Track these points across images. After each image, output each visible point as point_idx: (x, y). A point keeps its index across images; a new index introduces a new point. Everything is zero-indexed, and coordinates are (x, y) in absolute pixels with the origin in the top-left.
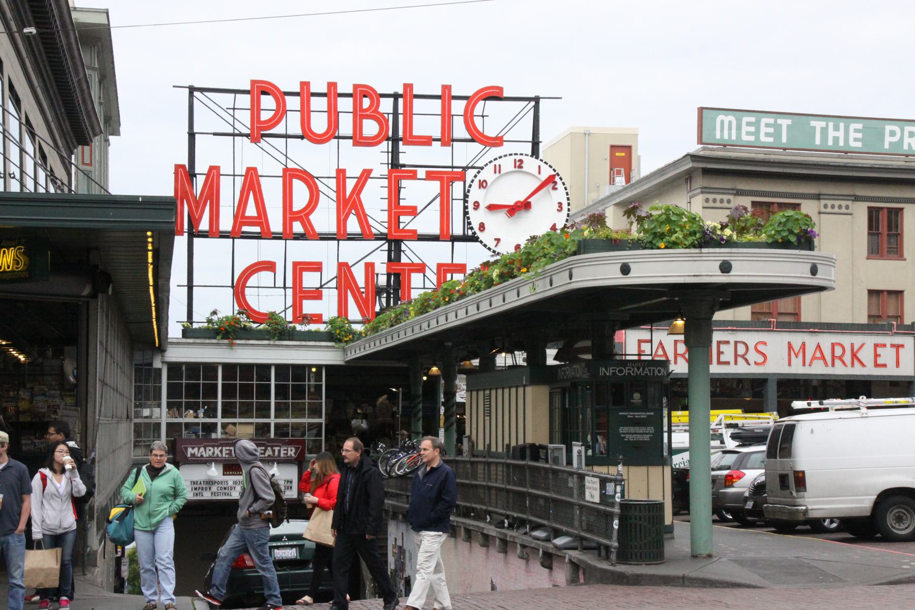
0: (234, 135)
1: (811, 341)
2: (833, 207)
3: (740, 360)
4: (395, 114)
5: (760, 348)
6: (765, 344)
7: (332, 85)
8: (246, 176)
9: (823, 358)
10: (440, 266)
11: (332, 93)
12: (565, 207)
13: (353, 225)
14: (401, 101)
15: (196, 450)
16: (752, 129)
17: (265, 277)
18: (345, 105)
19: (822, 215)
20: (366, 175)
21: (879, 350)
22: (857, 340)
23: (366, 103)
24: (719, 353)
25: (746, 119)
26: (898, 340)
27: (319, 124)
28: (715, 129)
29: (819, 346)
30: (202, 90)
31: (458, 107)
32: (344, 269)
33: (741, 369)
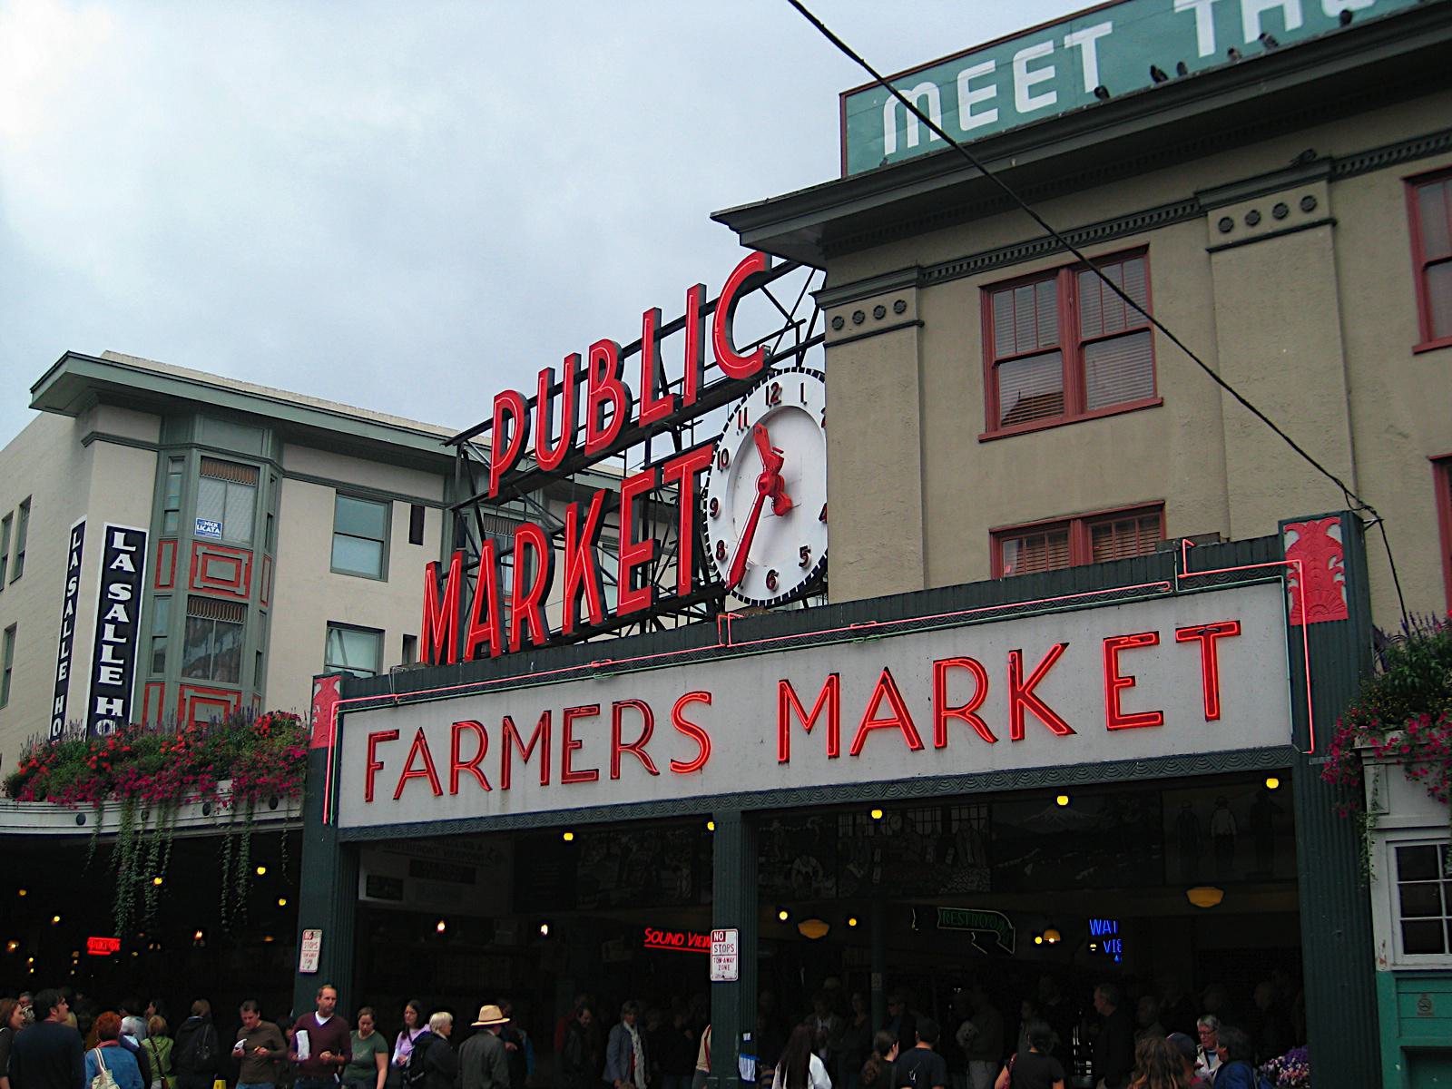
1: (858, 669)
2: (1254, 219)
3: (629, 762)
5: (691, 714)
6: (706, 698)
9: (903, 720)
16: (990, 92)
19: (1216, 257)
21: (1128, 663)
22: (1034, 637)
24: (571, 746)
25: (965, 76)
26: (1208, 609)
28: (882, 134)
29: (887, 682)
33: (633, 788)
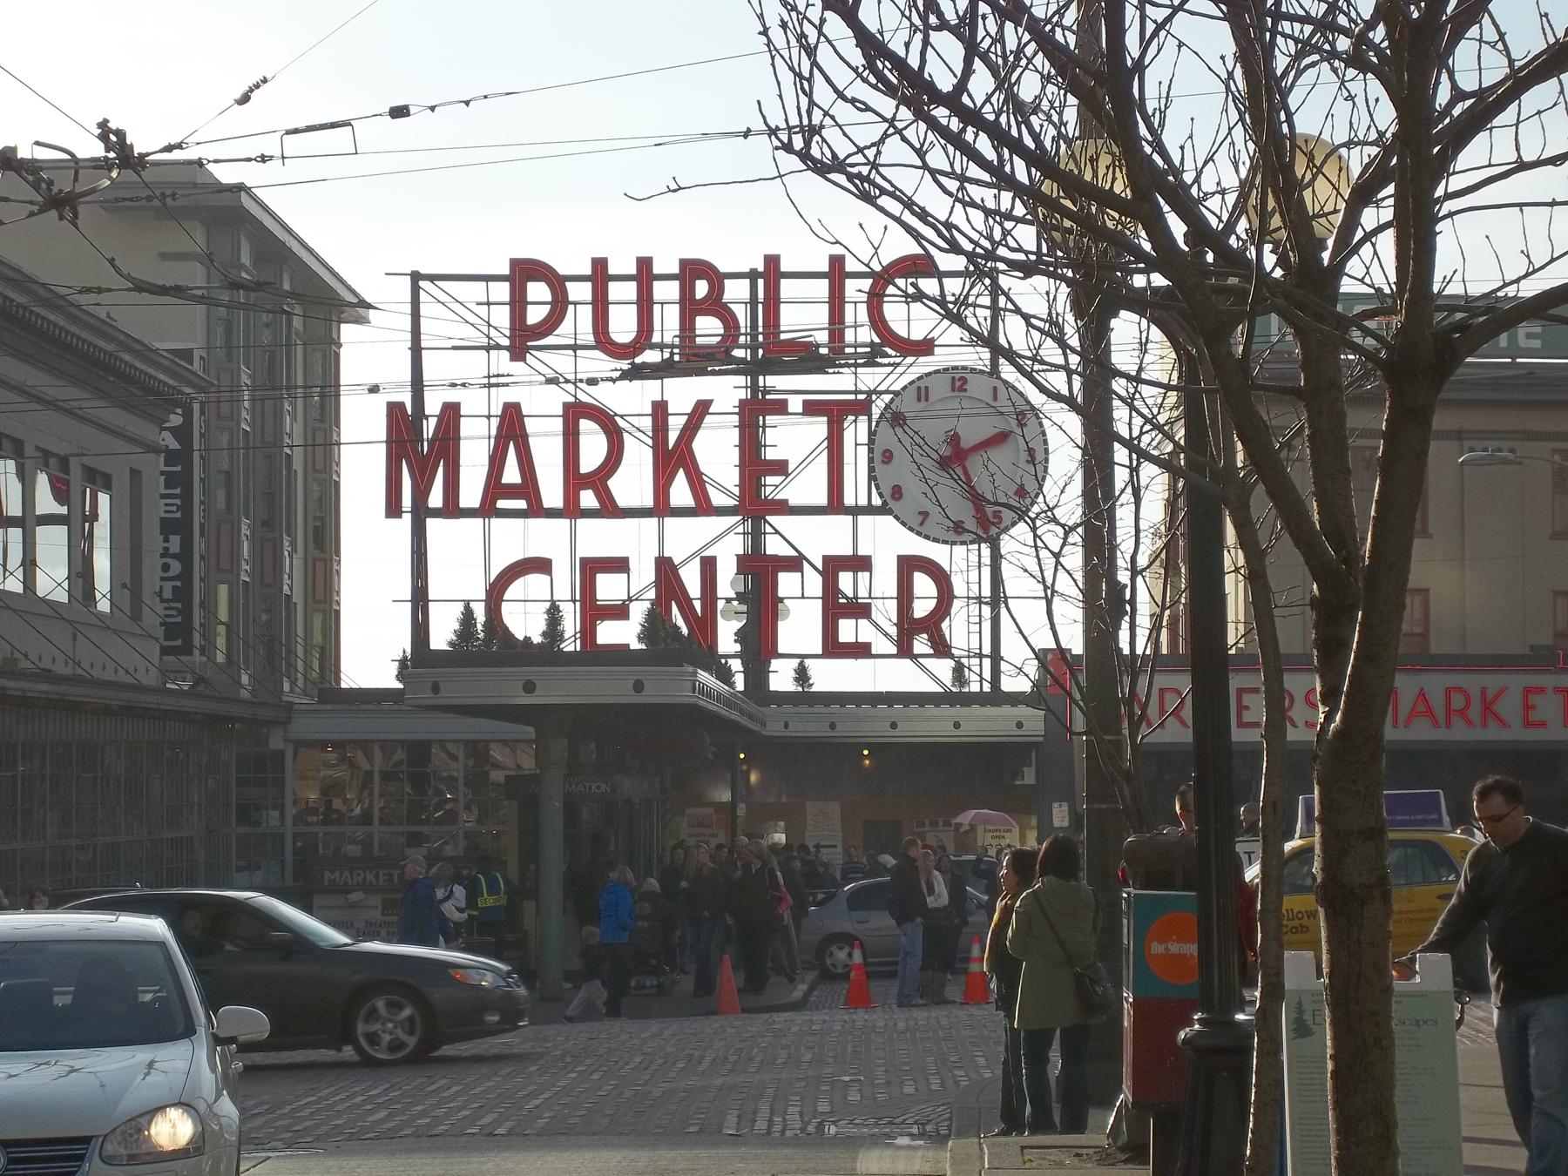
0: (488, 348)
4: (753, 301)
7: (645, 264)
8: (503, 417)
9: (1430, 712)
10: (826, 559)
11: (645, 274)
12: (1040, 456)
13: (681, 493)
14: (761, 282)
15: (337, 874)
17: (533, 584)
18: (666, 291)
20: (702, 409)
21: (1534, 699)
22: (1493, 681)
23: (702, 288)
27: (623, 325)
29: (1422, 695)
30: (433, 278)
31: (856, 290)
32: (666, 570)
